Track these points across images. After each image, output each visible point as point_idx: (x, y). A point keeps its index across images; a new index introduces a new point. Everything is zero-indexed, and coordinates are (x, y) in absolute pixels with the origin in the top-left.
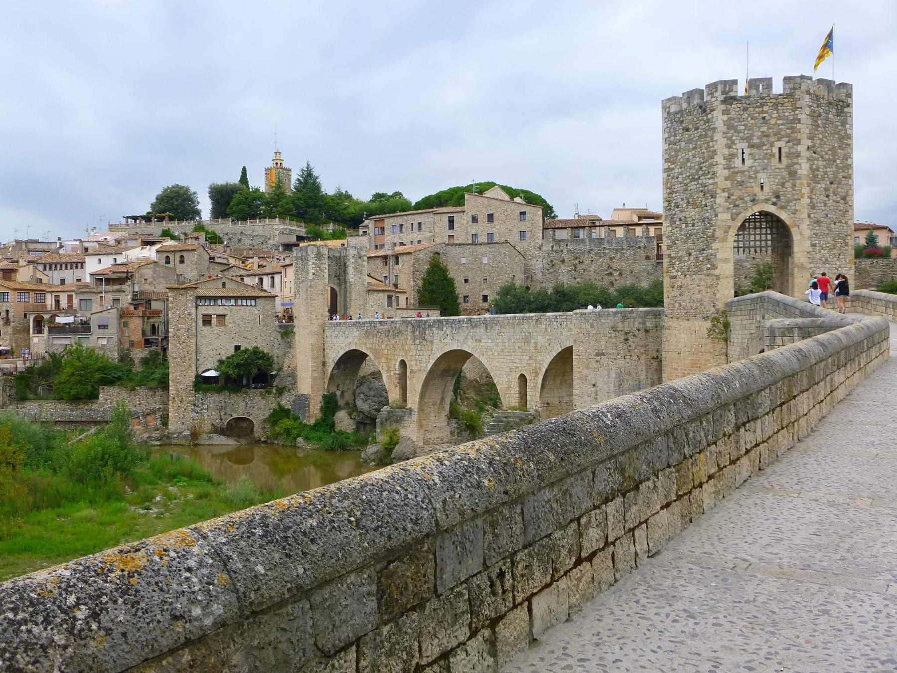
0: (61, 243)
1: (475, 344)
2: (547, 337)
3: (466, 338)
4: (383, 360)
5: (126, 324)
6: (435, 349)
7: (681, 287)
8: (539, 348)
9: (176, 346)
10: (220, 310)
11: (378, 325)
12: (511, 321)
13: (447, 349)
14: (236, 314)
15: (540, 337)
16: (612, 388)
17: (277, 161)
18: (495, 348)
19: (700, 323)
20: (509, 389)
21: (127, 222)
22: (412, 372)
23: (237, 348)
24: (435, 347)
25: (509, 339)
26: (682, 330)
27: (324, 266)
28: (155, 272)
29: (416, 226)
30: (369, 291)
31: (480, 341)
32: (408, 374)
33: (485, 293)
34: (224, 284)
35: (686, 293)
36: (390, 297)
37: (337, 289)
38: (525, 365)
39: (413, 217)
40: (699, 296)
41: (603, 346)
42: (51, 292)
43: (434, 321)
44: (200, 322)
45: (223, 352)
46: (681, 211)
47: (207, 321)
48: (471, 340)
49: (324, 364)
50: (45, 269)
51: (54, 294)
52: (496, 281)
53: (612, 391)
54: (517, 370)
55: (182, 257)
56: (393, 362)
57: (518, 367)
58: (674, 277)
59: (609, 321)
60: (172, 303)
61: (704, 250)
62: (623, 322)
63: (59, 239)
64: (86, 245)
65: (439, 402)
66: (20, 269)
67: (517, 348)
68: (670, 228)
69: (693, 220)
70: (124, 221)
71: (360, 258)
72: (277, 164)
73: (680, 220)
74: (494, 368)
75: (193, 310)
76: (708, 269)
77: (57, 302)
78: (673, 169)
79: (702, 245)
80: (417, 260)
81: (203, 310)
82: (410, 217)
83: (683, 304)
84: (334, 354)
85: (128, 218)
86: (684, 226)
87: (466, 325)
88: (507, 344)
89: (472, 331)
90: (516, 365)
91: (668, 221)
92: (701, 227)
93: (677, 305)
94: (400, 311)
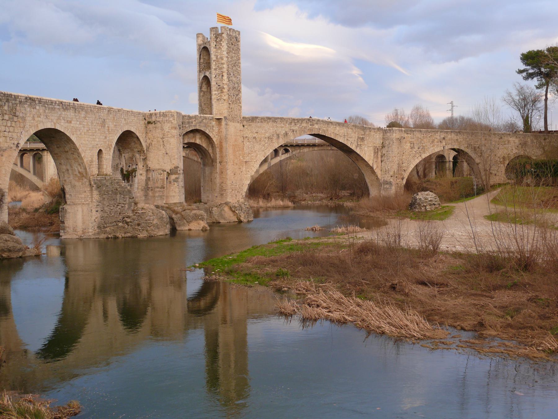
1: (67, 124)
2: (115, 124)
3: (59, 118)
6: (27, 126)
8: (110, 131)
12: (92, 109)
13: (41, 127)
15: (110, 123)
18: (82, 129)
20: (92, 161)
25: (92, 123)
31: (70, 122)
38: (102, 143)
43: (26, 98)
48: (63, 121)
54: (97, 146)
57: (97, 145)
58: (229, 104)
67: (97, 130)
74: (81, 145)
79: (237, 93)
87: (58, 107)
88: (90, 127)
89: (63, 113)
90: (96, 143)
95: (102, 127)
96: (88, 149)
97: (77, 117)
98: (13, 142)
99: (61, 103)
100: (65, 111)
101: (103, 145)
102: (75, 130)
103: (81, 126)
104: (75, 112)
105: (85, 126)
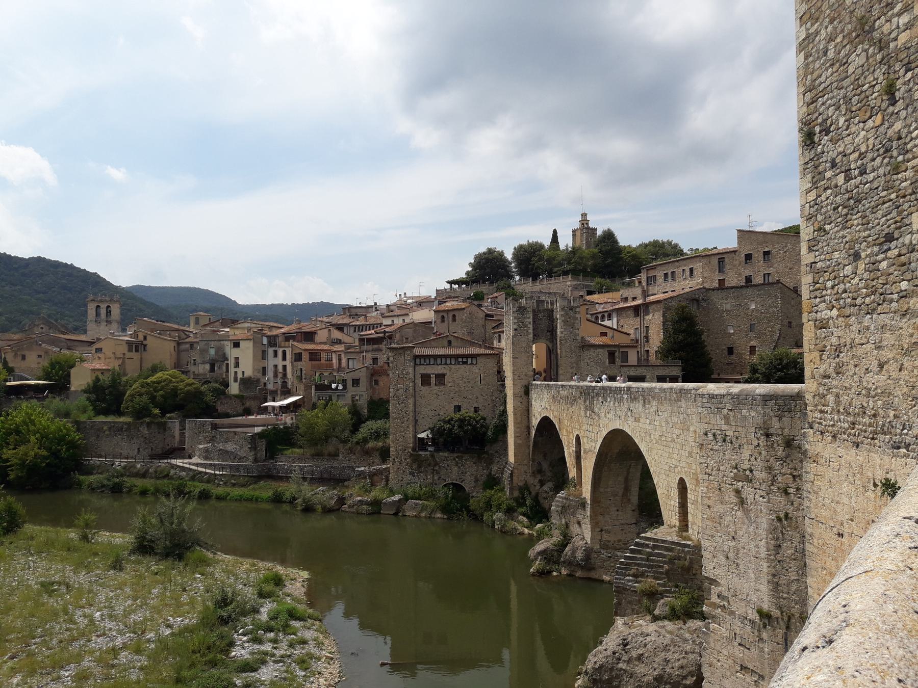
0: (376, 308)
4: (565, 433)
5: (376, 382)
6: (601, 424)
7: (838, 350)
9: (396, 407)
10: (439, 369)
11: (561, 389)
14: (455, 374)
16: (763, 553)
17: (582, 222)
19: (887, 459)
21: (451, 286)
22: (585, 452)
23: (458, 408)
24: (602, 422)
26: (844, 472)
27: (528, 320)
28: (415, 331)
29: (688, 273)
30: (583, 346)
32: (582, 451)
33: (753, 343)
34: (450, 343)
35: (851, 367)
36: (612, 355)
37: (550, 346)
39: (685, 262)
40: (881, 379)
41: (746, 462)
42: (335, 351)
44: (419, 381)
45: (442, 413)
46: (834, 141)
47: (426, 379)
48: (630, 419)
49: (528, 428)
50: (355, 331)
51: (338, 353)
52: (766, 329)
53: (763, 556)
54: (676, 469)
55: (454, 316)
56: (571, 436)
57: (676, 466)
58: (822, 325)
59: (753, 413)
60: (392, 363)
61: (890, 238)
62: (780, 418)
63: (376, 304)
64: (392, 308)
65: (621, 493)
66: (318, 332)
67: (675, 436)
68: (812, 196)
69: (862, 156)
70: (448, 286)
71: (571, 309)
72: (583, 224)
73: (834, 165)
74: (653, 463)
75: (411, 370)
76: (904, 295)
77: (340, 360)
78: (817, 33)
80: (667, 309)
81: (422, 370)
82: (681, 262)
83: (844, 399)
84: (535, 422)
85: (451, 283)
86: (841, 179)
87: (625, 396)
91: (809, 176)
92: (881, 171)
93: (831, 398)
94: (626, 369)
95: (683, 430)
96: (663, 472)
97: (647, 412)
98: (592, 444)
99: (629, 388)
100: (633, 403)
101: (686, 469)
102: (643, 434)
103: (650, 427)
104: (645, 403)
105: (658, 428)
